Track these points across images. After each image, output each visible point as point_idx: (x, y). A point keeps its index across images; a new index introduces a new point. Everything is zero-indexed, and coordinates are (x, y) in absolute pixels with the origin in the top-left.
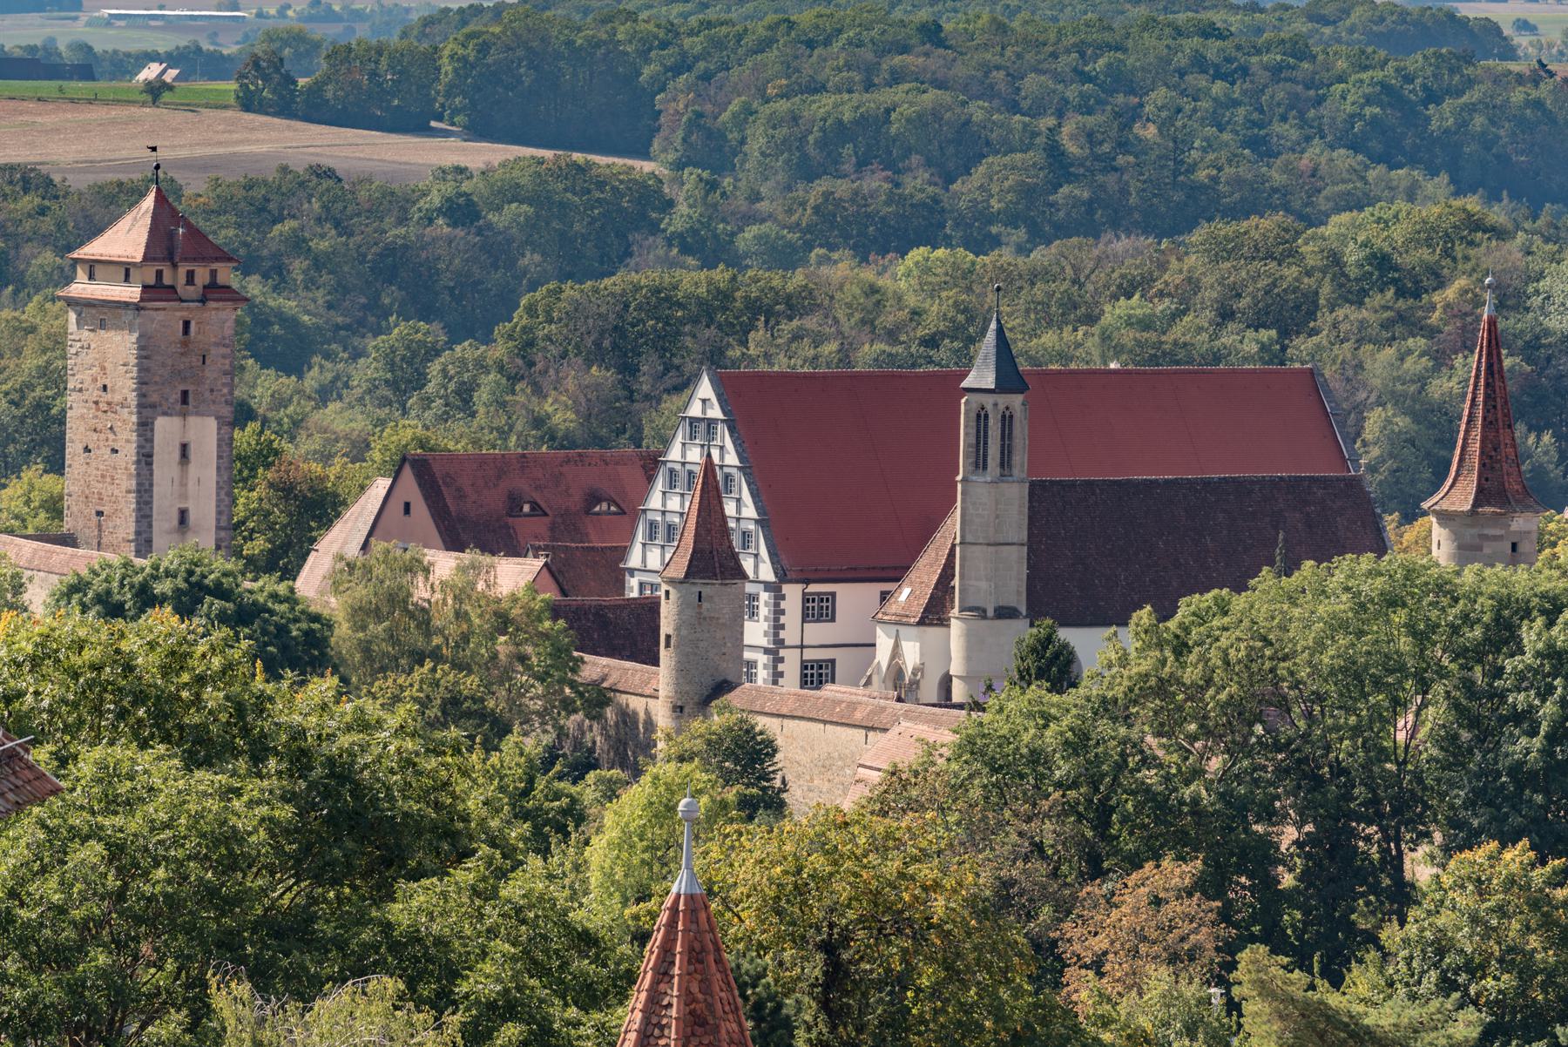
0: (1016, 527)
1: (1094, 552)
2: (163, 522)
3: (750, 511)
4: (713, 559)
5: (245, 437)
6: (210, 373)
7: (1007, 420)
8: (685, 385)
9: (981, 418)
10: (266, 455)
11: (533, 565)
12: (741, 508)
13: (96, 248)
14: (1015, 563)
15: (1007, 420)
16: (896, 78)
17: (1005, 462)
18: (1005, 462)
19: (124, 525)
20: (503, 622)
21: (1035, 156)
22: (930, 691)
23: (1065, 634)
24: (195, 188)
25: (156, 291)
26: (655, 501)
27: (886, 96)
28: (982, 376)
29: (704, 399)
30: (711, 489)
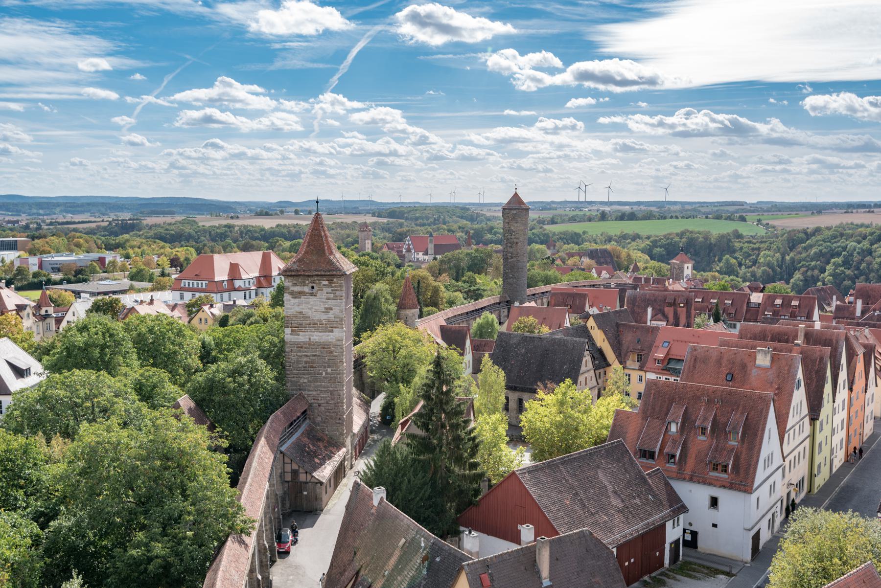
4: (409, 250)
30: (409, 245)
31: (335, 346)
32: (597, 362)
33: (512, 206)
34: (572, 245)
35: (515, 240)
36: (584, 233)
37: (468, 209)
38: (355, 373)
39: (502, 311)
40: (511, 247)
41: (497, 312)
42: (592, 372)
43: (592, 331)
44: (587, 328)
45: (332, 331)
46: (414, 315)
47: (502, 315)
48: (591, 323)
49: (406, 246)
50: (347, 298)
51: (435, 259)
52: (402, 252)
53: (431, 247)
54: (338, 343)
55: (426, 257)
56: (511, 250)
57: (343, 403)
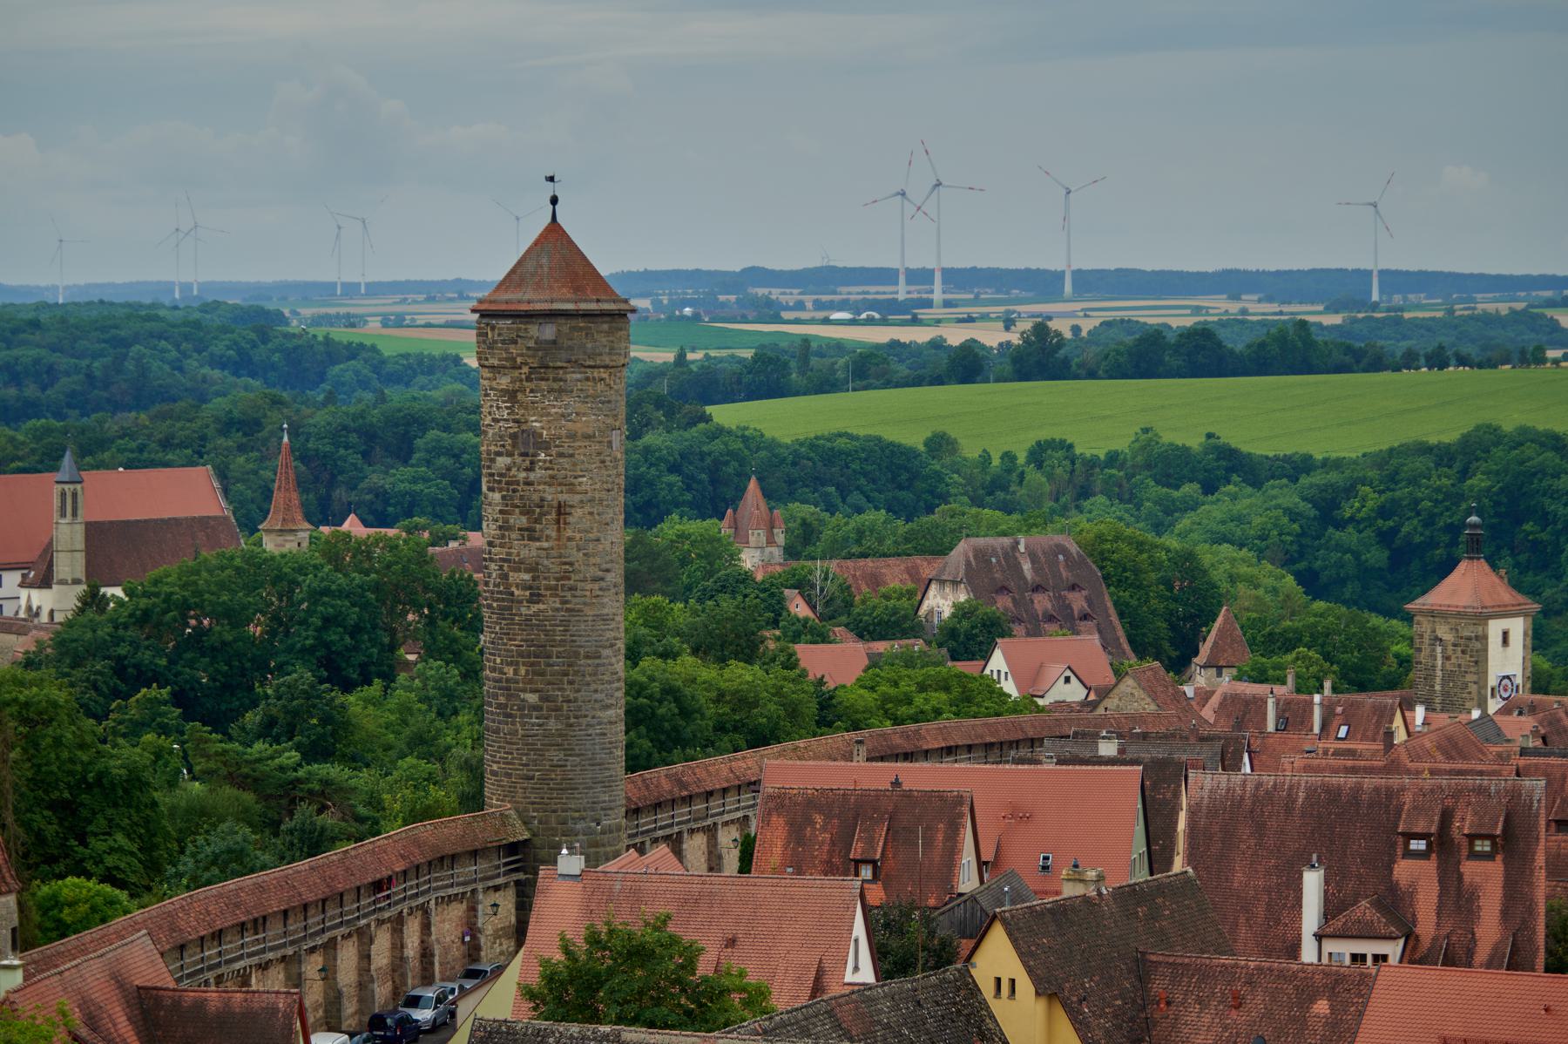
0: (80, 544)
7: (75, 495)
14: (80, 558)
15: (75, 495)
17: (74, 514)
18: (74, 514)
21: (81, 376)
27: (16, 352)
35: (550, 494)
36: (940, 444)
39: (485, 902)
40: (530, 534)
41: (457, 911)
43: (1000, 1009)
47: (489, 924)
48: (996, 959)
53: (69, 537)
55: (41, 599)
56: (529, 551)
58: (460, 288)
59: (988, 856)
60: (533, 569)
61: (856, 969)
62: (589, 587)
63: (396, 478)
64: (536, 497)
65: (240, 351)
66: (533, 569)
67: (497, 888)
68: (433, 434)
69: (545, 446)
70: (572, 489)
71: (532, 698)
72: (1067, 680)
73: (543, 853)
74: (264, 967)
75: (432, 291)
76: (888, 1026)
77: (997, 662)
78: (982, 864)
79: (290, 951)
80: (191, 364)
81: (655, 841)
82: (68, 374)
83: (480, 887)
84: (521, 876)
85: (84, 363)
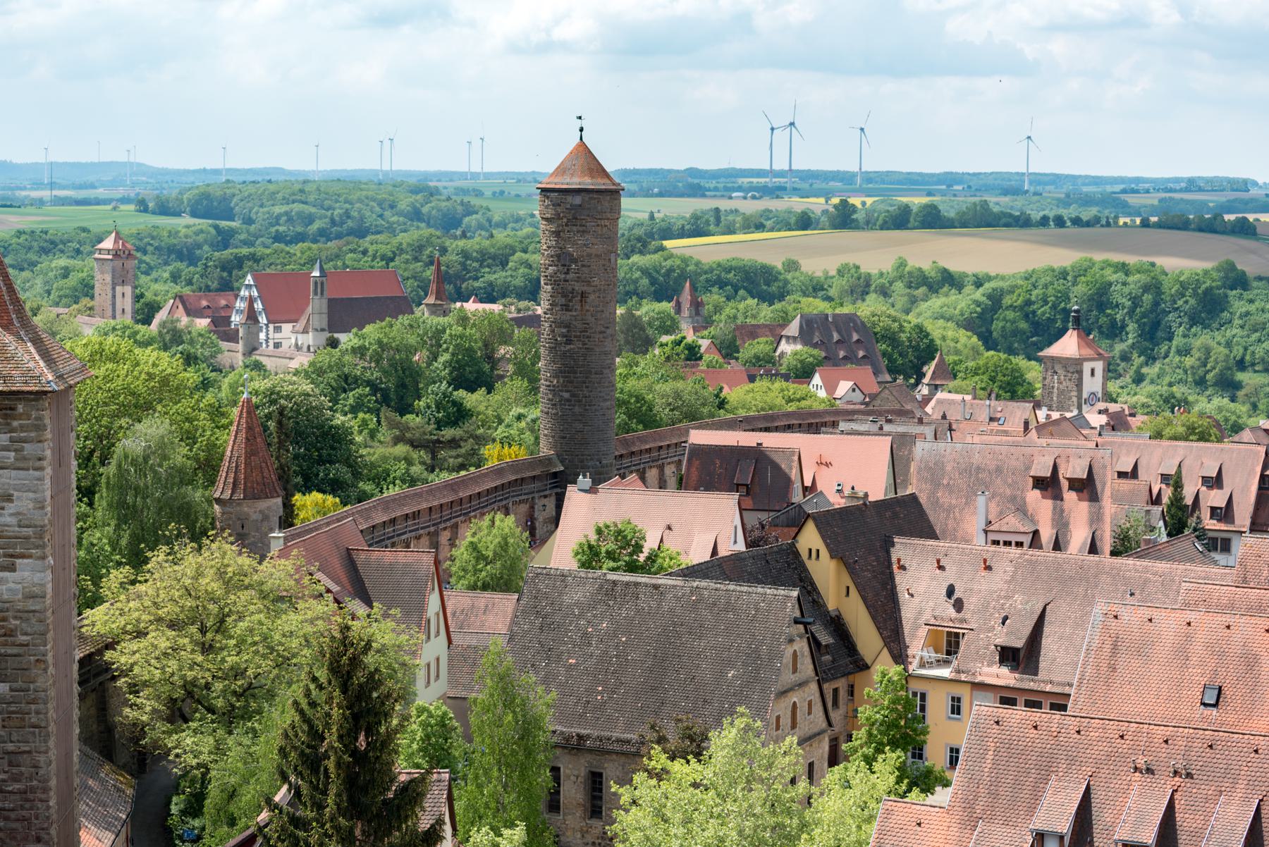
0: (325, 310)
1: (342, 314)
2: (118, 312)
3: (261, 306)
4: (252, 316)
5: (137, 291)
6: (129, 276)
7: (322, 284)
8: (244, 276)
9: (316, 283)
10: (142, 296)
11: (208, 320)
12: (258, 306)
13: (101, 246)
14: (325, 317)
15: (322, 284)
16: (294, 202)
19: (109, 313)
20: (200, 335)
21: (327, 220)
22: (305, 349)
23: (336, 335)
24: (125, 231)
25: (116, 255)
26: (238, 304)
27: (291, 206)
28: (316, 273)
29: (249, 279)
30: (251, 301)
31: (23, 614)
32: (827, 658)
33: (574, 182)
34: (751, 302)
35: (578, 287)
37: (432, 193)
38: (82, 697)
39: (539, 503)
42: (814, 687)
43: (811, 565)
44: (797, 554)
45: (12, 568)
46: (266, 518)
47: (540, 516)
48: (810, 539)
49: (240, 305)
50: (60, 462)
51: (333, 343)
52: (227, 320)
54: (32, 605)
56: (567, 316)
57: (46, 790)
58: (534, 177)
59: (808, 483)
60: (568, 326)
61: (735, 542)
62: (597, 336)
63: (498, 277)
64: (570, 288)
65: (415, 208)
66: (568, 326)
67: (545, 497)
68: (519, 255)
69: (575, 261)
70: (589, 283)
71: (566, 395)
72: (854, 390)
73: (571, 478)
74: (418, 538)
75: (521, 178)
76: (750, 574)
77: (817, 380)
78: (805, 489)
79: (432, 529)
80: (387, 213)
81: (631, 472)
82: (320, 218)
83: (536, 495)
84: (559, 490)
85: (329, 213)
